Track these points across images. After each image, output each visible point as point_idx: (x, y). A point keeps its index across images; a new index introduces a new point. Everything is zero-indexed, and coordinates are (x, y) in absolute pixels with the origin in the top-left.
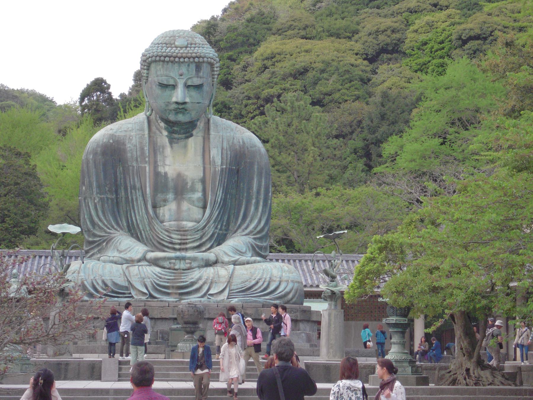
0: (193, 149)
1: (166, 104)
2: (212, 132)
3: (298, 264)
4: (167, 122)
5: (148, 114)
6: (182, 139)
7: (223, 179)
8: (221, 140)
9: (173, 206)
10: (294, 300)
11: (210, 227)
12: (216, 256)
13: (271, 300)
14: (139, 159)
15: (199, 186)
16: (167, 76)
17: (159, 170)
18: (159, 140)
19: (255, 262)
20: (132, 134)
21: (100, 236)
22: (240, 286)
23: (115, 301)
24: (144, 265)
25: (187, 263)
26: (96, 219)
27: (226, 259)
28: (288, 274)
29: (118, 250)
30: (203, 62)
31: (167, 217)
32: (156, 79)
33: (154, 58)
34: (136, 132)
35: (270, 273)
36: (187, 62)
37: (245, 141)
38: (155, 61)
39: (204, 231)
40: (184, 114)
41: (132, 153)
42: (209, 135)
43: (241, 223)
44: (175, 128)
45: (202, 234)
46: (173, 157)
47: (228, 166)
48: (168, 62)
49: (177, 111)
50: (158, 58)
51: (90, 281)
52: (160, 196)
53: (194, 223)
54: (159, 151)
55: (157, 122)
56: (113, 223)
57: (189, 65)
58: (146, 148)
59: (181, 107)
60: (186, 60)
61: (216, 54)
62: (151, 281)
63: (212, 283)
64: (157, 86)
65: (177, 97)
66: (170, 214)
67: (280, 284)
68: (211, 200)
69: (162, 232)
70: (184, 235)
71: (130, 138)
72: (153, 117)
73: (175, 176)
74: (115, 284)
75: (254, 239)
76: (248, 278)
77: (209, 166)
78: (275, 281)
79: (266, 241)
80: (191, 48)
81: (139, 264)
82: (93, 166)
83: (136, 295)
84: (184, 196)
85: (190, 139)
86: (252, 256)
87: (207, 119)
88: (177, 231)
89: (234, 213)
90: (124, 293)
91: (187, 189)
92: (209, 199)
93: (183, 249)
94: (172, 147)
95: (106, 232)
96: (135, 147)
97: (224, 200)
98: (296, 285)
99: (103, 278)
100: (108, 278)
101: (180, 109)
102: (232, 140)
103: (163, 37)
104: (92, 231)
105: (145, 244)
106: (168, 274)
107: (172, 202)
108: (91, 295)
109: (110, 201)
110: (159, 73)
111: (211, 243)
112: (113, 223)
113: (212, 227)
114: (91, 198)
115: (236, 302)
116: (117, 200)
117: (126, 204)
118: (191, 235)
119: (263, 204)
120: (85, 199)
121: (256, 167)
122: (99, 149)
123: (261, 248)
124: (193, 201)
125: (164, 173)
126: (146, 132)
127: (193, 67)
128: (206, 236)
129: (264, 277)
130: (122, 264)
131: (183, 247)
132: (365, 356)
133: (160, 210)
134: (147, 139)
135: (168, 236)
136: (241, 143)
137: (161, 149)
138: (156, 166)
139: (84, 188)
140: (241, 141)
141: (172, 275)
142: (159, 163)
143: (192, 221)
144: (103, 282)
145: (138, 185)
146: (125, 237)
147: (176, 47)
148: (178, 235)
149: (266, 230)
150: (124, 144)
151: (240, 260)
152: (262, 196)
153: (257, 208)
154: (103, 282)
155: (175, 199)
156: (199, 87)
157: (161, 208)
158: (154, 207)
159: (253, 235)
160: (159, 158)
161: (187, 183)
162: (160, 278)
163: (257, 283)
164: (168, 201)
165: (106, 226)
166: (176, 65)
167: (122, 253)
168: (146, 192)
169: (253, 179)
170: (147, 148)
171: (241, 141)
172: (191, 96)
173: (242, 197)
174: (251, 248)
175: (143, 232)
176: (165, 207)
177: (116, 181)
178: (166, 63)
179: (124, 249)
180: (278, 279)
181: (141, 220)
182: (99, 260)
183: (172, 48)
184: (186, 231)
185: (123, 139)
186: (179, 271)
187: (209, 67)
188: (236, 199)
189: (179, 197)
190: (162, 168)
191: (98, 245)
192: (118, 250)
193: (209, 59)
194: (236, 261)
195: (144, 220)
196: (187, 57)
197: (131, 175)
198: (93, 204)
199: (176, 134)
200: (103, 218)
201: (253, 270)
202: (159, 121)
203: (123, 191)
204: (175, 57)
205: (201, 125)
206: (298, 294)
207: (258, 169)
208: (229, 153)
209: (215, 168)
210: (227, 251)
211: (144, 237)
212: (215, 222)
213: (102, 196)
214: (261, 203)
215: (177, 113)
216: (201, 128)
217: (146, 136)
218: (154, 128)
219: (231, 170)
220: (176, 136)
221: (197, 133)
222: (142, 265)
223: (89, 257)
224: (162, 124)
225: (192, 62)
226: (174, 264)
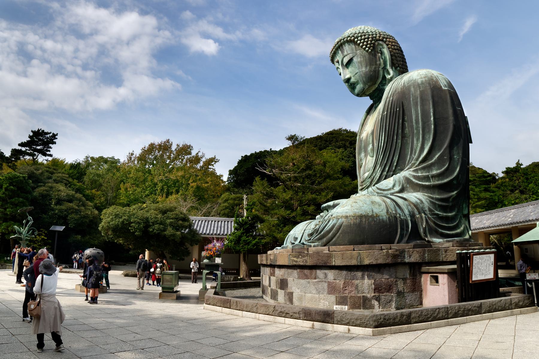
10: (334, 239)
39: (372, 177)
43: (410, 158)
67: (329, 222)
98: (340, 221)
123: (427, 178)
127: (340, 52)
132: (347, 324)
159: (416, 167)
206: (340, 232)
207: (413, 100)
208: (391, 98)
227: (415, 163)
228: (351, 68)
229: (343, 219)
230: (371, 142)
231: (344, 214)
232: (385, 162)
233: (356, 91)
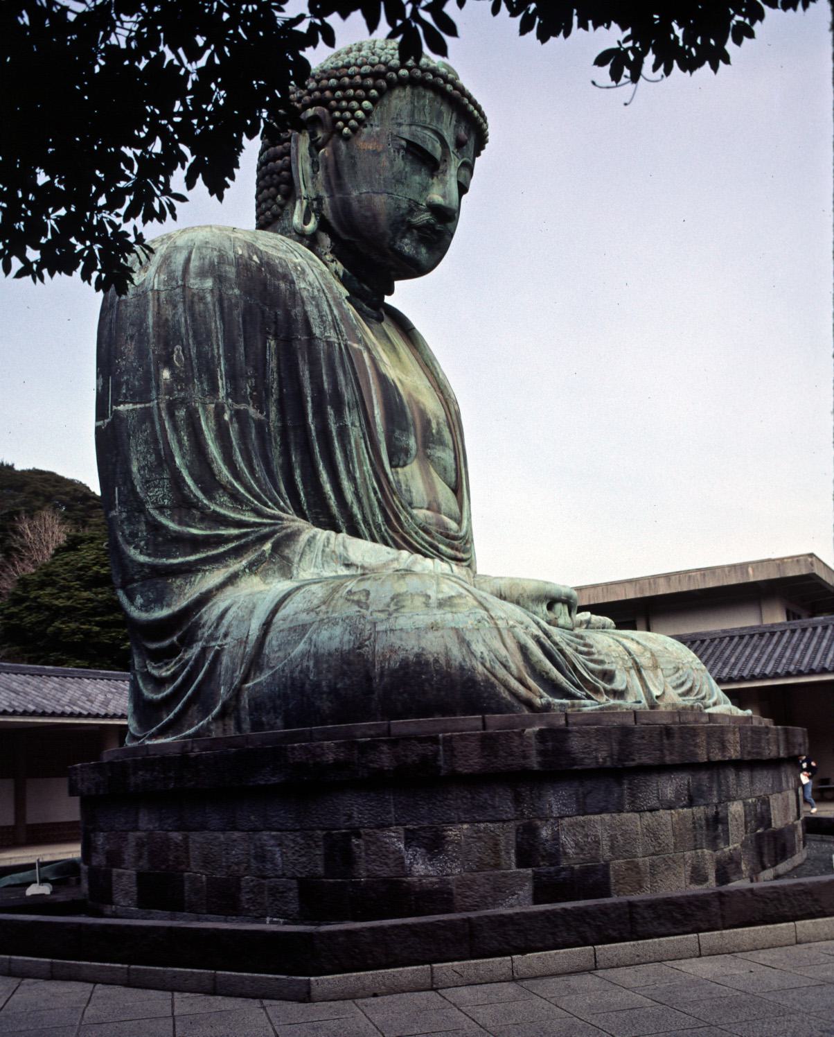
6: (372, 317)
16: (436, 133)
21: (239, 524)
26: (225, 473)
32: (405, 131)
44: (366, 287)
59: (438, 227)
64: (402, 151)
84: (429, 451)
91: (432, 434)
95: (259, 513)
104: (202, 509)
114: (204, 405)
120: (172, 407)
139: (166, 374)
143: (451, 517)
145: (348, 395)
148: (448, 545)
157: (399, 470)
161: (429, 422)
181: (356, 493)
191: (237, 552)
198: (212, 424)
202: (329, 257)
230: (451, 445)
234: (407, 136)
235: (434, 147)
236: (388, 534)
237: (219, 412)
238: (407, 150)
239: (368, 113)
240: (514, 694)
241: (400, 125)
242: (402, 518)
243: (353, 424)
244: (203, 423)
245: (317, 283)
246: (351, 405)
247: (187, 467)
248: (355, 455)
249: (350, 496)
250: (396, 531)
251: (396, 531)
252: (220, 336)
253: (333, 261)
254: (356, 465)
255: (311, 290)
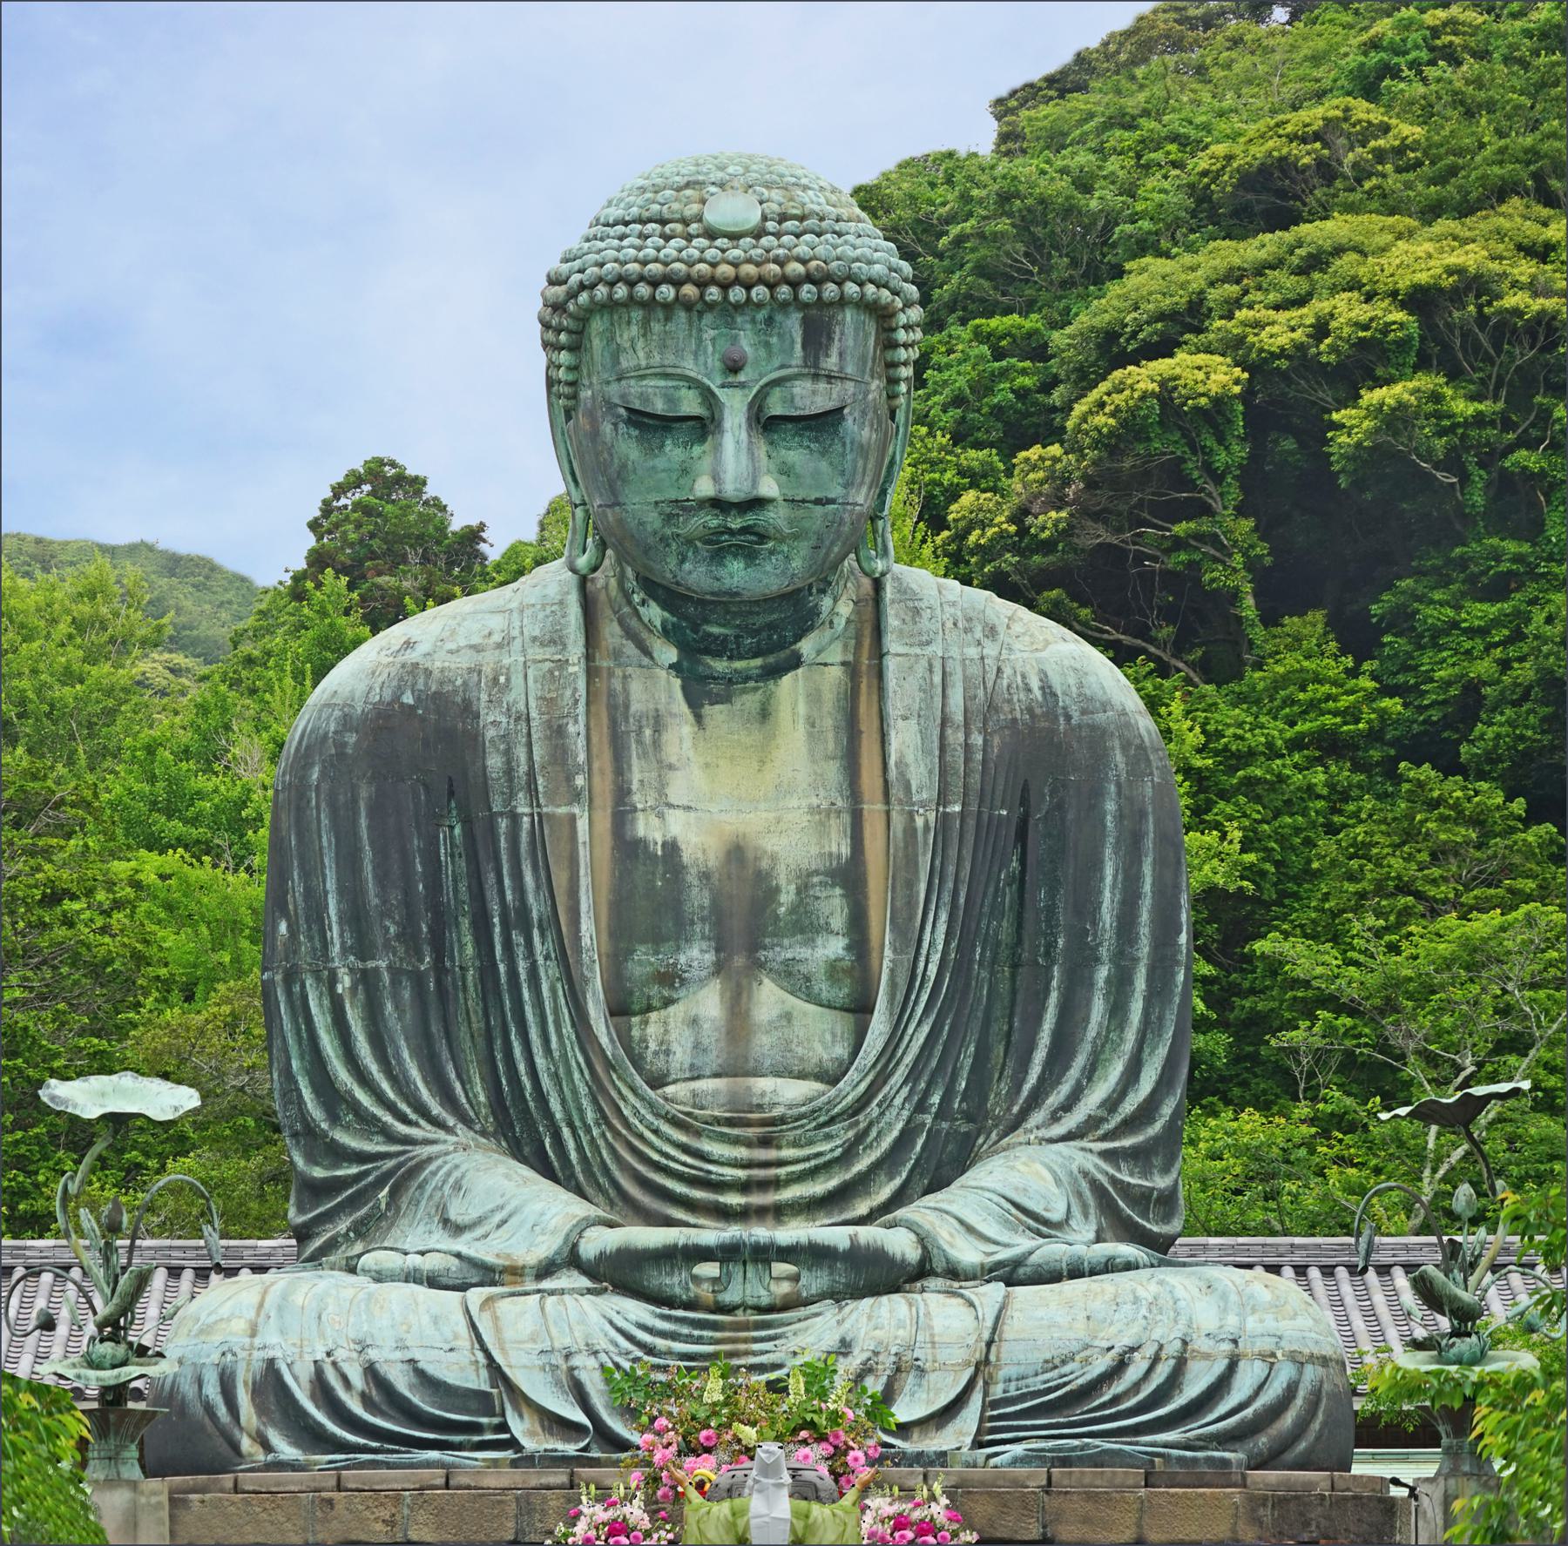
0: (802, 728)
1: (668, 510)
2: (892, 644)
3: (1346, 1289)
4: (669, 596)
5: (582, 562)
6: (747, 679)
7: (951, 869)
8: (937, 679)
9: (708, 1002)
10: (1302, 1446)
11: (886, 1105)
12: (922, 1240)
13: (1187, 1447)
14: (540, 781)
15: (833, 907)
16: (666, 376)
17: (641, 831)
18: (636, 687)
19: (1109, 1267)
20: (506, 661)
22: (1036, 1384)
23: (428, 1464)
24: (572, 1291)
25: (778, 1279)
26: (343, 1076)
27: (968, 1254)
28: (1270, 1324)
29: (446, 1222)
30: (842, 302)
31: (681, 1056)
32: (614, 390)
33: (601, 291)
34: (524, 651)
35: (1183, 1321)
36: (760, 305)
37: (1056, 683)
38: (610, 306)
40: (751, 557)
41: (508, 753)
42: (881, 656)
43: (1041, 1079)
44: (715, 630)
45: (851, 1134)
46: (707, 765)
47: (974, 808)
48: (668, 307)
49: (719, 547)
50: (621, 291)
51: (306, 1371)
52: (644, 960)
53: (818, 1086)
54: (639, 742)
55: (630, 602)
56: (425, 1094)
57: (770, 321)
58: (576, 728)
59: (736, 523)
60: (759, 292)
61: (906, 267)
62: (602, 1366)
63: (898, 1370)
64: (621, 425)
65: (716, 478)
66: (697, 1046)
68: (892, 971)
69: (656, 1132)
70: (765, 1142)
71: (495, 680)
72: (605, 579)
73: (713, 861)
74: (426, 1380)
75: (1107, 1155)
76: (1075, 1346)
77: (880, 807)
78: (1207, 1356)
79: (1165, 1170)
80: (778, 235)
81: (546, 1284)
82: (325, 821)
83: (531, 1434)
84: (762, 954)
85: (787, 680)
86: (1099, 1239)
87: (866, 583)
88: (730, 1123)
89: (1009, 1034)
90: (476, 1428)
91: (777, 916)
92: (886, 964)
93: (761, 1213)
94: (699, 718)
95: (391, 1137)
96: (523, 725)
97: (958, 967)
98: (1311, 1373)
99: (373, 1354)
100: (398, 1355)
101: (731, 532)
102: (991, 676)
103: (643, 190)
104: (325, 1134)
105: (581, 1193)
106: (685, 1330)
107: (702, 982)
108: (315, 1438)
109: (407, 994)
110: (626, 362)
111: (898, 1182)
112: (425, 1094)
113: (898, 1101)
115: (1015, 1461)
116: (439, 982)
117: (484, 999)
118: (795, 1144)
119: (1150, 980)
121: (1110, 806)
122: (352, 738)
123: (1142, 1199)
124: (808, 979)
125: (664, 845)
126: (576, 651)
127: (793, 324)
128: (870, 1146)
129: (1156, 1335)
130: (463, 1288)
131: (757, 1199)
133: (646, 1023)
134: (581, 684)
135: (685, 1149)
136: (1038, 694)
137: (648, 732)
138: (622, 813)
139: (283, 927)
140: (1035, 684)
141: (705, 1333)
142: (637, 799)
143: (802, 1076)
144: (371, 1371)
146: (479, 1157)
147: (711, 234)
148: (736, 1141)
149: (1167, 1110)
150: (468, 710)
151: (1034, 1259)
152: (1144, 949)
153: (1117, 1011)
154: (371, 1371)
155: (719, 969)
156: (823, 424)
157: (653, 1016)
158: (619, 1010)
160: (638, 773)
162: (650, 1350)
163: (1120, 1366)
164: (683, 981)
165: (391, 1107)
166: (708, 318)
167: (467, 1236)
168: (577, 937)
169: (1096, 865)
170: (581, 727)
171: (1035, 684)
172: (785, 471)
173: (1047, 954)
174: (1091, 1201)
175: (566, 1132)
176: (671, 1009)
177: (435, 885)
178: (661, 315)
179: (473, 1214)
180: (1227, 1347)
181: (555, 1077)
182: (352, 1270)
183: (689, 238)
184: (772, 1122)
185: (465, 683)
186: (740, 1316)
187: (871, 328)
188: (1015, 966)
189: (739, 961)
190: (654, 821)
191: (353, 1203)
192: (446, 1222)
193: (870, 289)
194: (1017, 1262)
195: (569, 1073)
196: (761, 280)
197: (504, 858)
198: (326, 1002)
199: (717, 654)
200: (374, 1068)
201: (1097, 1305)
203: (468, 939)
204: (702, 283)
205: (841, 608)
206: (1320, 1416)
207: (1120, 817)
208: (977, 739)
209: (911, 816)
210: (972, 1220)
211: (573, 1156)
212: (913, 1075)
213: (371, 964)
214: (1140, 984)
215: (718, 556)
216: (840, 623)
217: (577, 668)
218: (611, 632)
219: (986, 829)
220: (720, 666)
221: (819, 652)
222: (562, 1292)
223: (312, 1258)
224: (654, 613)
225: (784, 306)
226: (715, 1281)
227: (1102, 1120)
228: (795, 456)
229: (1320, 1370)
230: (838, 922)
231: (1316, 1352)
232: (934, 1063)
233: (736, 574)
234: (617, 401)
235: (671, 400)
236: (606, 1140)
237: (333, 980)
238: (629, 422)
239: (570, 369)
240: (235, 1447)
241: (608, 383)
242: (626, 1112)
243: (547, 957)
244: (312, 1004)
245: (522, 707)
246: (545, 924)
247: (308, 1073)
248: (548, 1011)
249: (546, 1082)
250: (617, 1134)
251: (617, 1134)
252: (326, 861)
253: (643, 603)
254: (552, 1028)
255: (504, 720)
